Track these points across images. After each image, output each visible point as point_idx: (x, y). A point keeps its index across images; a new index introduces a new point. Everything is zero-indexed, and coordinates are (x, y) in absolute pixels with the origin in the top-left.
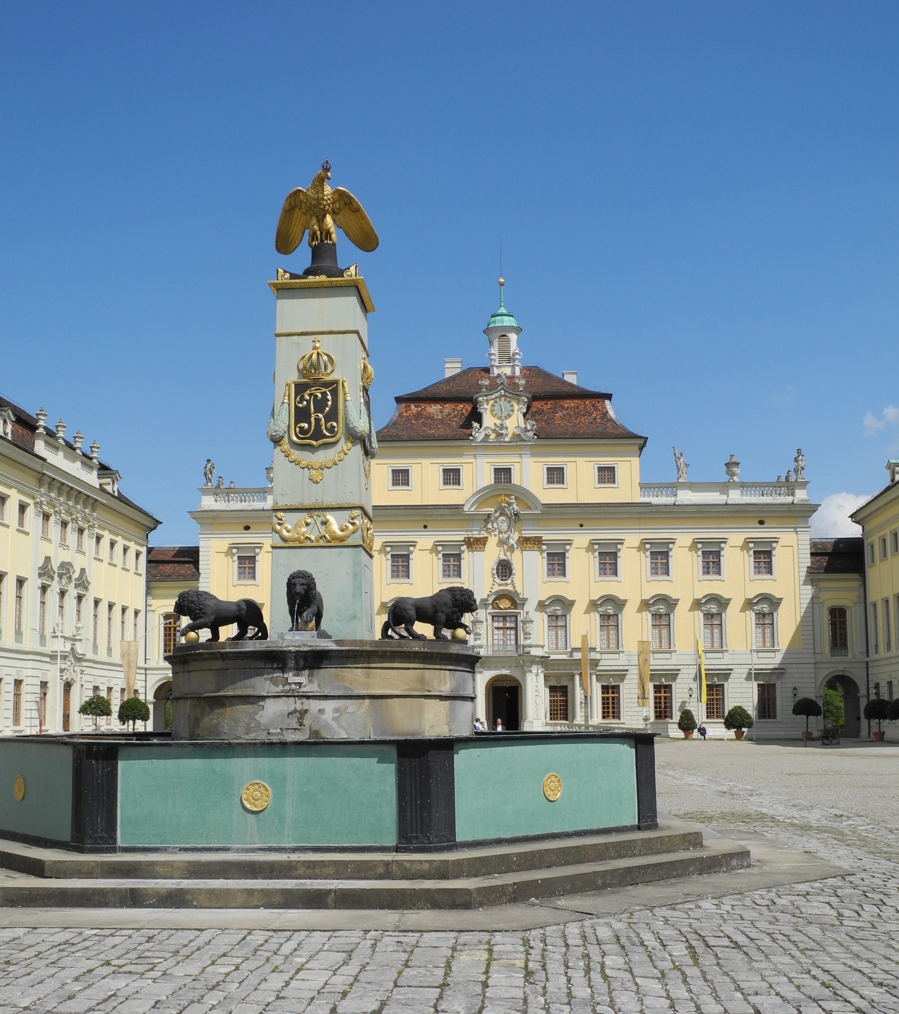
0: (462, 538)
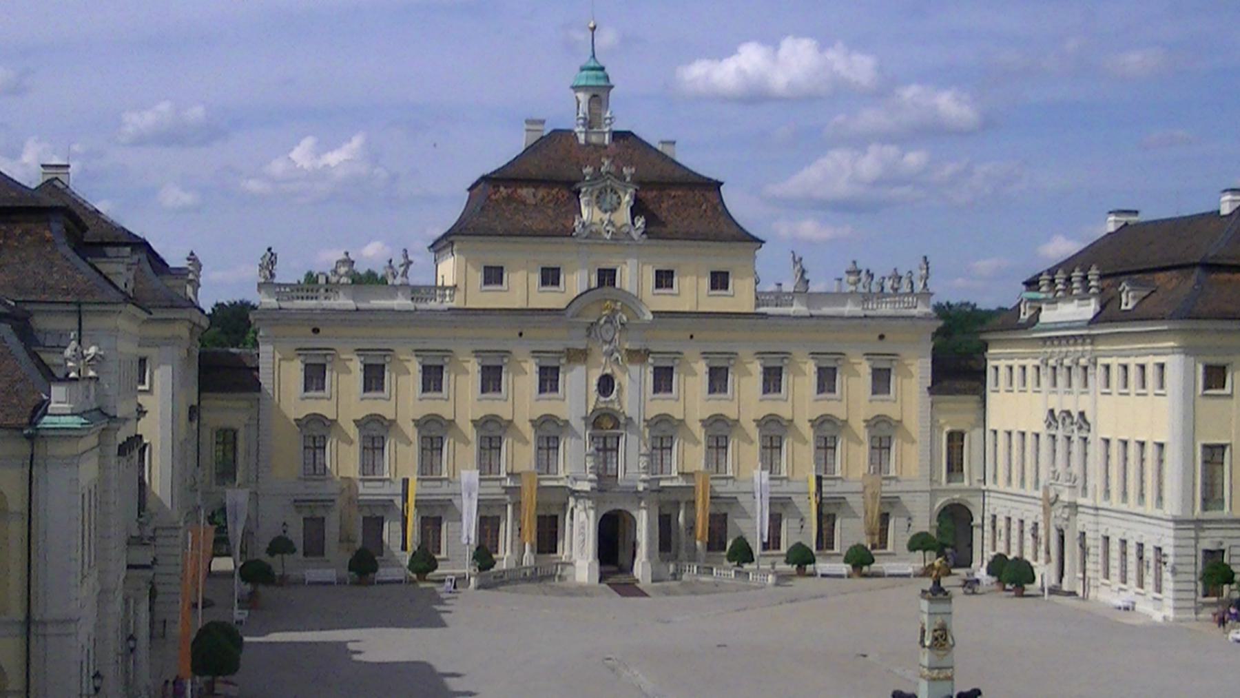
0: (561, 348)
